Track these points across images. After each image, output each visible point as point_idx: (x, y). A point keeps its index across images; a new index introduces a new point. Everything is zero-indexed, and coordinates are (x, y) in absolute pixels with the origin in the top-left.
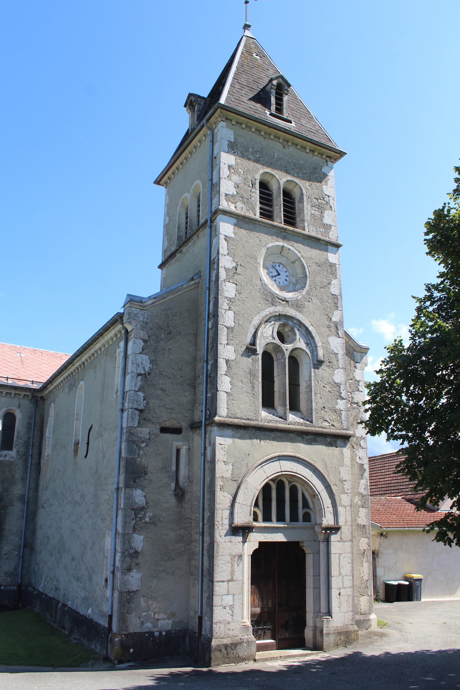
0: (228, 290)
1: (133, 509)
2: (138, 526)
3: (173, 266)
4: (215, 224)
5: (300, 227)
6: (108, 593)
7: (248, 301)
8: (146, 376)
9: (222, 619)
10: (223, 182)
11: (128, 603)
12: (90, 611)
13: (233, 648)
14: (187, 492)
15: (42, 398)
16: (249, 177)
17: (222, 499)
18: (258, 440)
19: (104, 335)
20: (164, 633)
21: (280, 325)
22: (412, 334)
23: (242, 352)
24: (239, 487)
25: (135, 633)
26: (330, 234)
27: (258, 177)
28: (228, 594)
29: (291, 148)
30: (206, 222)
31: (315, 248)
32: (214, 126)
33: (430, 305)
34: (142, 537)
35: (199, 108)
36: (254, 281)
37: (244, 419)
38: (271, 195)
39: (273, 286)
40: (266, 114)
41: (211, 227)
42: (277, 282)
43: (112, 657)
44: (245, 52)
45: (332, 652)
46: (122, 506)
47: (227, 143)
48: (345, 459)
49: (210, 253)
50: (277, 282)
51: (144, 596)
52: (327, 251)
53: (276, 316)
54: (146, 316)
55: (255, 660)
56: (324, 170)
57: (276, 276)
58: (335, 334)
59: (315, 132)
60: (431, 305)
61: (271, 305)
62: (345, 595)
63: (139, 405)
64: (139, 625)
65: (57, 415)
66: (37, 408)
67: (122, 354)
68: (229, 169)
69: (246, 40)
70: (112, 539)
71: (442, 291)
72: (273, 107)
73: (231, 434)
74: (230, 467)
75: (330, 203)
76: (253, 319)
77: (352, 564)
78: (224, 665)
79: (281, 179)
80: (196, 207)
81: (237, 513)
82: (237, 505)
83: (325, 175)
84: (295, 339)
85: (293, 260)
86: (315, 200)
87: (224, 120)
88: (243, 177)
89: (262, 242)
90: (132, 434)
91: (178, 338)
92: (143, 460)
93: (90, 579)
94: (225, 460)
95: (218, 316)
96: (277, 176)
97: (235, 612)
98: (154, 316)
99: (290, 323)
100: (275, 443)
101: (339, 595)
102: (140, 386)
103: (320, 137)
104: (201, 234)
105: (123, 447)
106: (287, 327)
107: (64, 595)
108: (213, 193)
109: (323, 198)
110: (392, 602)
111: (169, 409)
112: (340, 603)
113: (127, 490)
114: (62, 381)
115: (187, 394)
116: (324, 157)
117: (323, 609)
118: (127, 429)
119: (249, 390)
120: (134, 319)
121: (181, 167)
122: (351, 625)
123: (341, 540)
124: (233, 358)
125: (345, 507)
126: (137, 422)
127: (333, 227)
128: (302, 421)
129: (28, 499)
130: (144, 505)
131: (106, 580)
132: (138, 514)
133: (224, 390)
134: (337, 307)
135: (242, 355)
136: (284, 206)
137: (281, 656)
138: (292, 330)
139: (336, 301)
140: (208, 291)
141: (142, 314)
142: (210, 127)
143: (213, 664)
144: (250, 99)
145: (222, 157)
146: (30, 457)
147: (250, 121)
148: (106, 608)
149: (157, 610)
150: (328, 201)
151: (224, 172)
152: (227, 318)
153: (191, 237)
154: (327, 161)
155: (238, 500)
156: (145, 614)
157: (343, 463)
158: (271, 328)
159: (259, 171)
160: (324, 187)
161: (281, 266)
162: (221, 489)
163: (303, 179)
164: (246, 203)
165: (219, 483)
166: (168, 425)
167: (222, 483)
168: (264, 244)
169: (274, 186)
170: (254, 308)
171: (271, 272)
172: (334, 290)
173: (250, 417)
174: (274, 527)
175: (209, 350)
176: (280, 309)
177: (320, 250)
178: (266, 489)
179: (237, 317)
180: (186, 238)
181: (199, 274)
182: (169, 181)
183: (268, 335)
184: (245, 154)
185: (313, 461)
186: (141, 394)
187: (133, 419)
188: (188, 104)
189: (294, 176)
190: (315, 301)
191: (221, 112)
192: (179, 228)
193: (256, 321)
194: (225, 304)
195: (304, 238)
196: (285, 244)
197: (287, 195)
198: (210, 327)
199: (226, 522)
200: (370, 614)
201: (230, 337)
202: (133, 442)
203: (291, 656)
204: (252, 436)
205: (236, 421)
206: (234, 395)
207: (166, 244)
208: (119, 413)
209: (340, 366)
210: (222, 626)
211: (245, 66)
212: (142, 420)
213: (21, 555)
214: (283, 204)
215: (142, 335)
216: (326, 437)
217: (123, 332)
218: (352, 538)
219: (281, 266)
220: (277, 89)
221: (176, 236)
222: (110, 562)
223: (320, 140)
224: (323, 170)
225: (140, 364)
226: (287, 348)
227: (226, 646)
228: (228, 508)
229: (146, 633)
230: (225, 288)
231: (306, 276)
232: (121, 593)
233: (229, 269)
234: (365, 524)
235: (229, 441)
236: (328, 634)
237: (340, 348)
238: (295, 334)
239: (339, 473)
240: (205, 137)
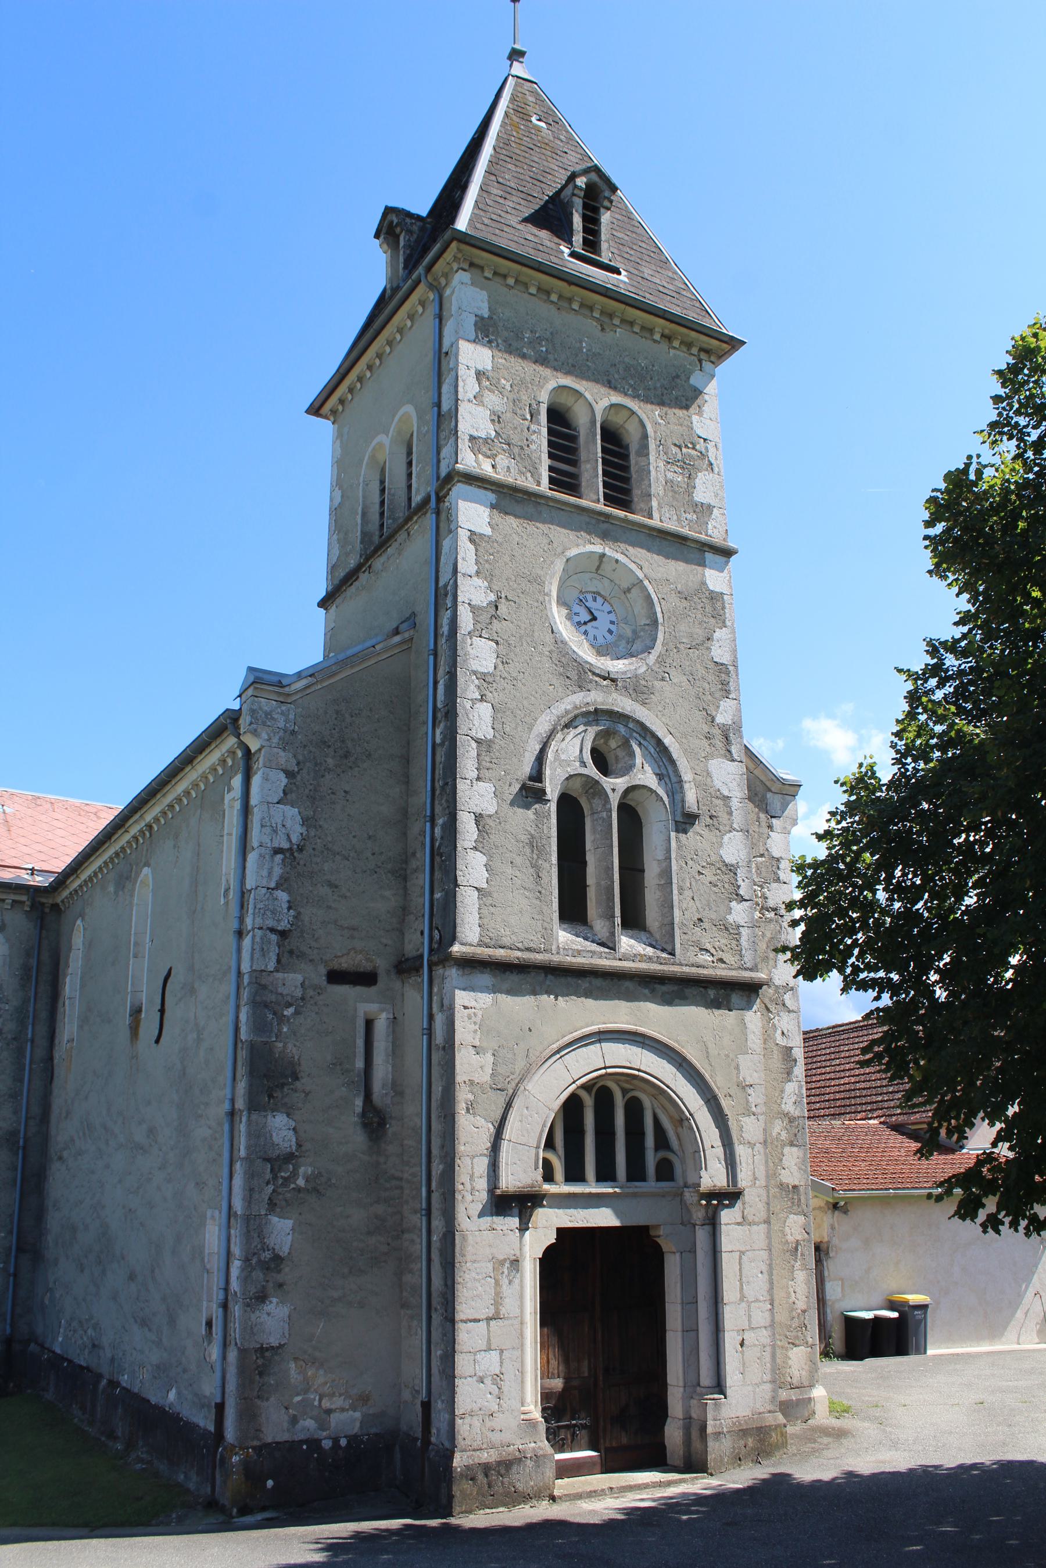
0: (478, 655)
1: (268, 1160)
2: (281, 1197)
3: (353, 601)
4: (447, 504)
5: (641, 510)
6: (214, 1353)
7: (524, 681)
8: (292, 854)
9: (475, 1407)
10: (464, 409)
11: (261, 1374)
12: (172, 1395)
13: (503, 1471)
14: (391, 1117)
15: (55, 907)
17: (472, 1132)
18: (552, 997)
19: (195, 762)
20: (343, 1442)
21: (598, 735)
22: (898, 752)
23: (512, 797)
24: (509, 1105)
25: (277, 1443)
26: (710, 526)
27: (544, 397)
28: (489, 1349)
29: (618, 330)
30: (426, 501)
31: (677, 559)
32: (443, 281)
33: (938, 687)
34: (289, 1223)
35: (409, 240)
36: (536, 634)
37: (519, 949)
38: (574, 439)
40: (563, 255)
41: (438, 513)
42: (591, 636)
43: (225, 1499)
44: (512, 111)
45: (726, 1476)
46: (243, 1153)
47: (472, 319)
48: (751, 1037)
49: (437, 571)
50: (591, 636)
51: (296, 1359)
52: (702, 564)
53: (588, 713)
54: (292, 716)
55: (553, 1498)
56: (695, 380)
57: (586, 622)
58: (722, 752)
59: (674, 294)
60: (941, 685)
62: (755, 1345)
63: (278, 921)
64: (285, 1425)
65: (89, 945)
66: (44, 932)
67: (238, 805)
68: (478, 379)
69: (516, 85)
70: (220, 1230)
71: (964, 654)
72: (578, 238)
73: (490, 984)
74: (489, 1058)
75: (710, 454)
76: (536, 719)
77: (771, 1274)
78: (482, 1512)
80: (404, 466)
81: (507, 1164)
82: (505, 1146)
83: (697, 393)
84: (632, 767)
85: (625, 585)
86: (675, 450)
87: (466, 267)
88: (511, 396)
89: (555, 545)
90: (264, 987)
92: (290, 1046)
93: (172, 1321)
94: (477, 1044)
95: (456, 715)
97: (505, 1389)
99: (622, 729)
100: (590, 1002)
101: (742, 1344)
102: (281, 877)
103: (685, 305)
104: (415, 527)
105: (243, 1017)
106: (614, 737)
107: (113, 1360)
108: (442, 435)
109: (692, 443)
110: (862, 1359)
111: (347, 928)
112: (744, 1364)
113: (254, 1116)
114: (100, 868)
115: (387, 893)
116: (695, 351)
117: (706, 1378)
118: (250, 977)
119: (530, 883)
120: (264, 724)
121: (368, 374)
122: (770, 1412)
123: (744, 1221)
124: (492, 810)
125: (752, 1145)
126: (274, 958)
127: (715, 510)
128: (650, 951)
129: (25, 1141)
130: (294, 1148)
131: (209, 1324)
132: (280, 1170)
133: (471, 883)
134: (728, 692)
135: (512, 804)
136: (605, 462)
137: (611, 1488)
138: (626, 744)
139: (724, 677)
140: (432, 658)
141: (282, 713)
142: (435, 283)
143: (456, 1509)
144: (526, 220)
145: (461, 353)
146: (29, 1044)
147: (525, 269)
148: (209, 1388)
149: (326, 1389)
150: (704, 451)
151: (468, 386)
152: (477, 719)
153: (392, 536)
154: (700, 361)
155: (507, 1134)
156: (299, 1398)
157: (746, 1046)
158: (577, 741)
159: (547, 383)
160: (695, 418)
161: (599, 600)
162: (468, 1110)
163: (647, 400)
164: (517, 457)
165: (463, 1096)
166: (345, 966)
167: (471, 1097)
168: (559, 550)
169: (581, 419)
170: (537, 696)
172: (720, 653)
173: (532, 945)
174: (590, 1194)
175: (438, 792)
176: (597, 697)
177: (687, 561)
178: (572, 1107)
180: (381, 537)
181: (411, 620)
182: (340, 408)
183: (570, 756)
184: (515, 344)
185: (677, 1041)
186: (283, 896)
187: (264, 953)
188: (384, 230)
189: (626, 395)
190: (677, 677)
191: (458, 249)
192: (364, 514)
193: (543, 725)
194: (472, 687)
195: (649, 535)
196: (607, 549)
197: (612, 437)
198: (438, 740)
199: (482, 1184)
200: (811, 1386)
201: (484, 763)
202: (266, 1006)
203: (635, 1486)
204: (538, 988)
205: (500, 954)
206: (495, 895)
207: (336, 552)
208: (232, 939)
209: (735, 826)
210: (476, 1422)
211: (513, 145)
212: (286, 955)
213: (12, 1270)
214: (603, 458)
215: (282, 761)
216: (705, 988)
217: (240, 754)
218: (769, 1217)
219: (599, 600)
220: (585, 197)
221: (359, 534)
222: (216, 1281)
223: (685, 311)
224: (692, 381)
225: (279, 826)
226: (615, 785)
227: (486, 1468)
228: (485, 1152)
229: (302, 1442)
230: (471, 651)
231: (655, 622)
232: (243, 1352)
233: (479, 608)
234: (797, 1183)
235: (485, 999)
236: (718, 1434)
237: (735, 783)
238: (632, 755)
239: (737, 1068)
240: (423, 307)
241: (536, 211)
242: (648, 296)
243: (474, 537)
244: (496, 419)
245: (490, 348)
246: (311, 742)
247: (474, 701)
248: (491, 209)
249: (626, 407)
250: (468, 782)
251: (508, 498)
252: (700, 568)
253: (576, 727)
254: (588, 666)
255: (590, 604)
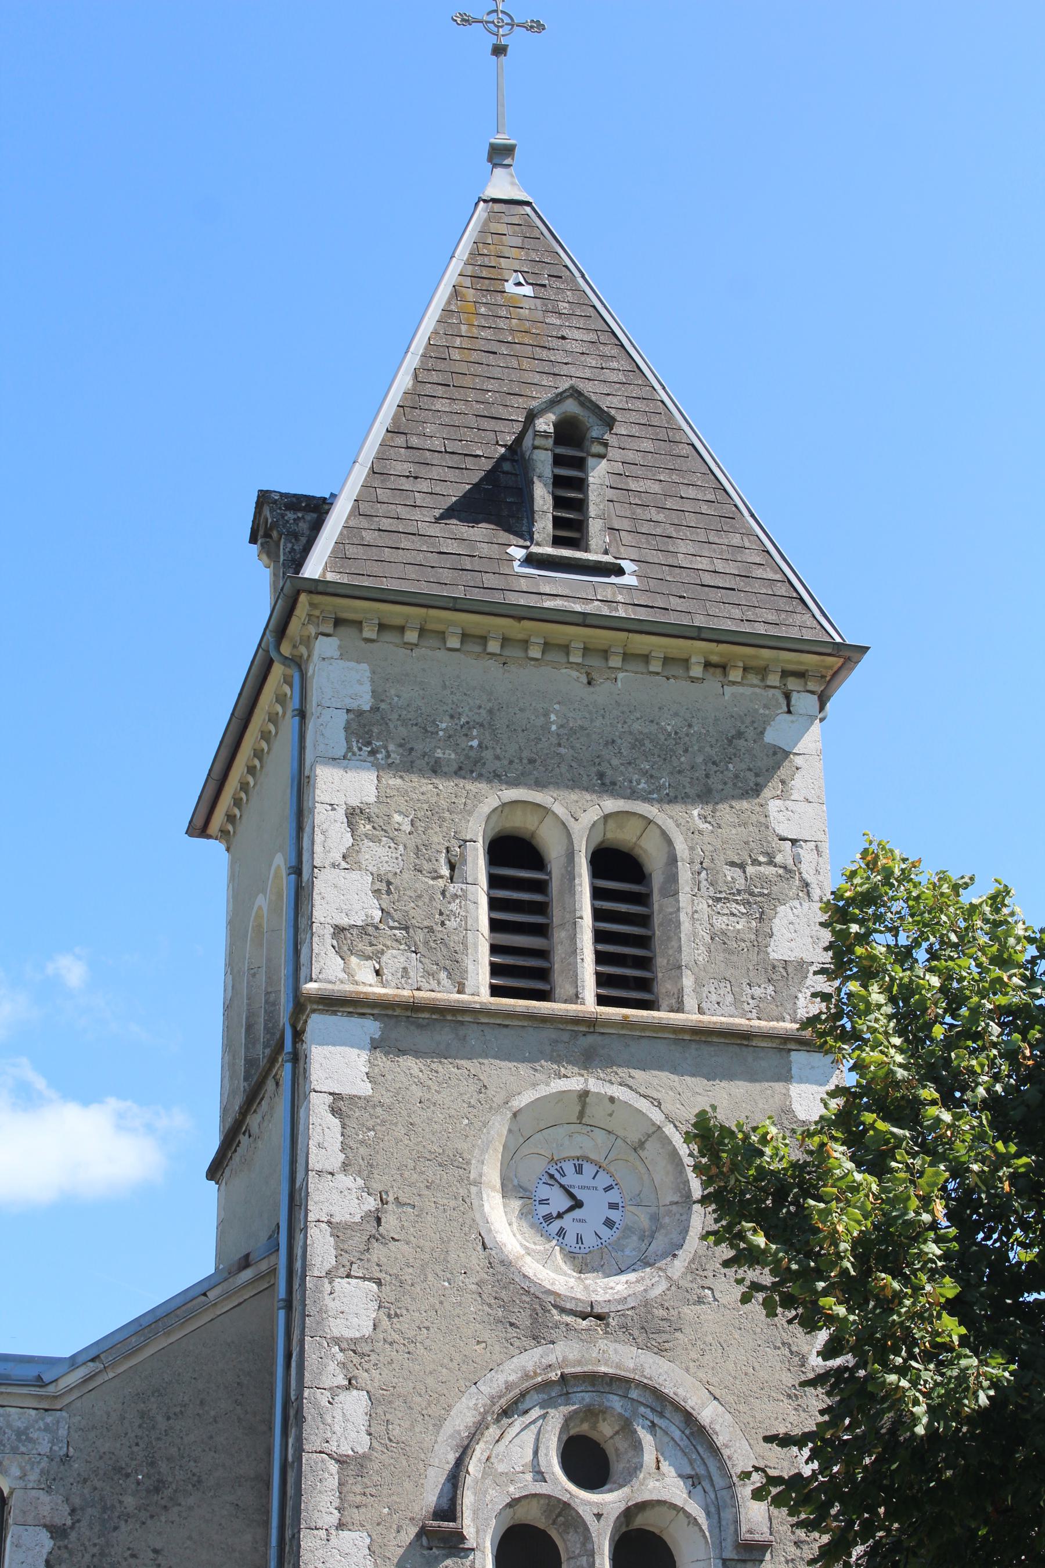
7: (428, 1342)
16: (438, 839)
21: (568, 1420)
23: (401, 1551)
31: (730, 1077)
35: (293, 550)
36: (452, 1256)
39: (546, 1259)
40: (511, 564)
42: (570, 1239)
44: (468, 282)
47: (342, 718)
50: (570, 1239)
52: (785, 1076)
53: (547, 1384)
54: (62, 1432)
61: (529, 1342)
68: (350, 824)
69: (489, 220)
72: (544, 526)
75: (804, 867)
79: (574, 820)
83: (780, 755)
84: (639, 1467)
85: (634, 1137)
86: (730, 873)
87: (329, 628)
89: (490, 1092)
91: (191, 1501)
96: (559, 809)
98: (94, 1427)
99: (616, 1403)
116: (774, 679)
120: (15, 1450)
138: (626, 1428)
140: (282, 1314)
141: (47, 1429)
144: (450, 513)
147: (433, 612)
150: (790, 862)
152: (339, 1420)
154: (787, 696)
158: (529, 1436)
164: (422, 949)
168: (499, 1100)
170: (453, 1365)
171: (542, 1202)
176: (568, 1353)
179: (380, 1411)
184: (419, 747)
191: (311, 604)
192: (249, 1028)
193: (463, 1415)
194: (332, 1367)
195: (676, 1041)
196: (592, 1081)
201: (351, 1497)
215: (45, 1511)
219: (589, 1169)
220: (557, 442)
224: (771, 736)
226: (601, 1507)
233: (347, 1226)
238: (637, 1446)
241: (476, 486)
242: (675, 603)
243: (339, 1106)
244: (383, 887)
245: (378, 767)
246: (96, 1472)
247: (334, 1391)
248: (381, 509)
249: (635, 814)
250: (322, 1533)
251: (405, 1026)
252: (779, 1086)
253: (526, 1412)
254: (551, 1299)
255: (570, 1179)
